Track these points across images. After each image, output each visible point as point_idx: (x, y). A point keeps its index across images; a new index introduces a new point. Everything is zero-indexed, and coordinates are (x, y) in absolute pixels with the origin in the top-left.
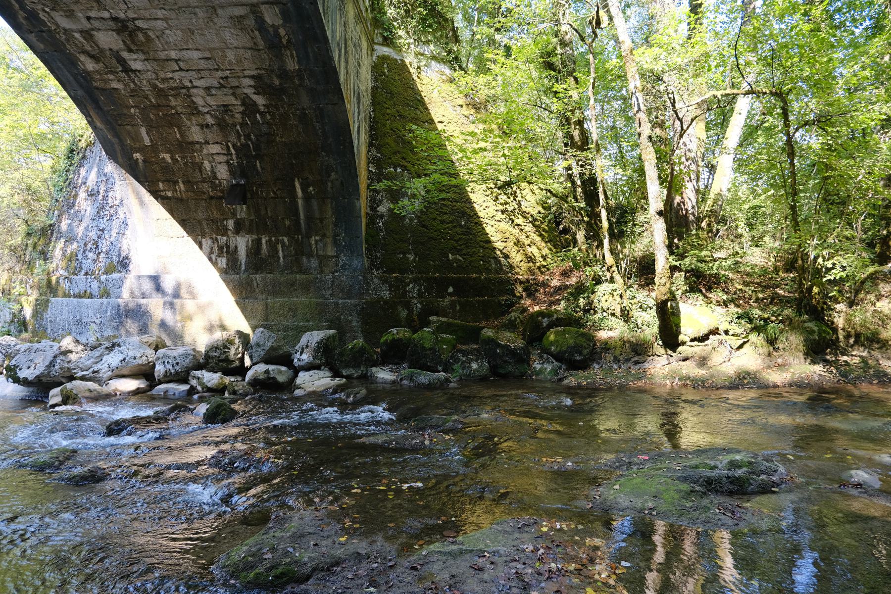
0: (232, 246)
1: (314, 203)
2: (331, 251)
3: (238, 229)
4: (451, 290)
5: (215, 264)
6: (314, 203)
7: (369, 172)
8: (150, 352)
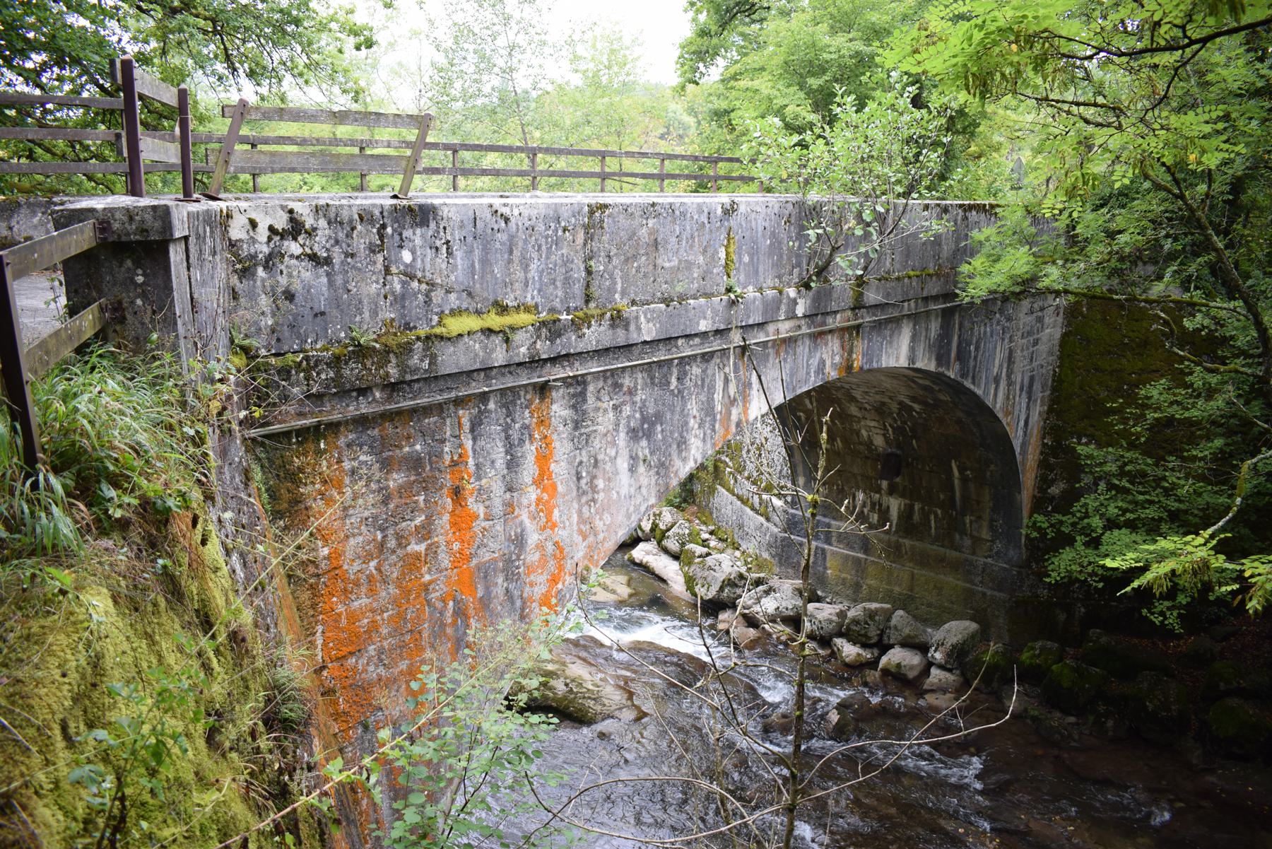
0: (884, 505)
1: (972, 486)
2: (985, 534)
3: (892, 491)
6: (972, 486)
7: (1044, 445)
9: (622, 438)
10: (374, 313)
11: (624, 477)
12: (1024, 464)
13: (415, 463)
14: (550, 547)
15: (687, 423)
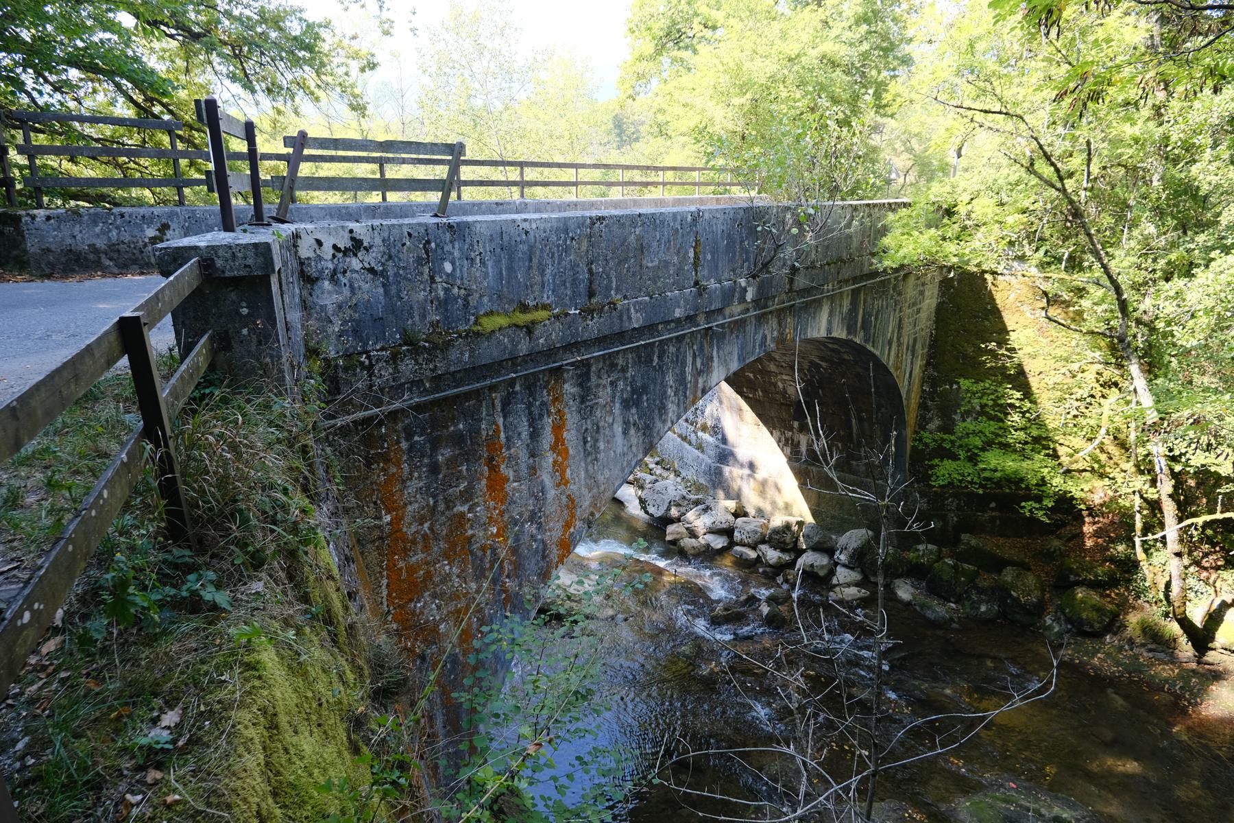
4: (993, 505)
5: (783, 450)
8: (731, 518)
10: (423, 316)
11: (619, 439)
12: (908, 406)
13: (458, 439)
15: (665, 392)
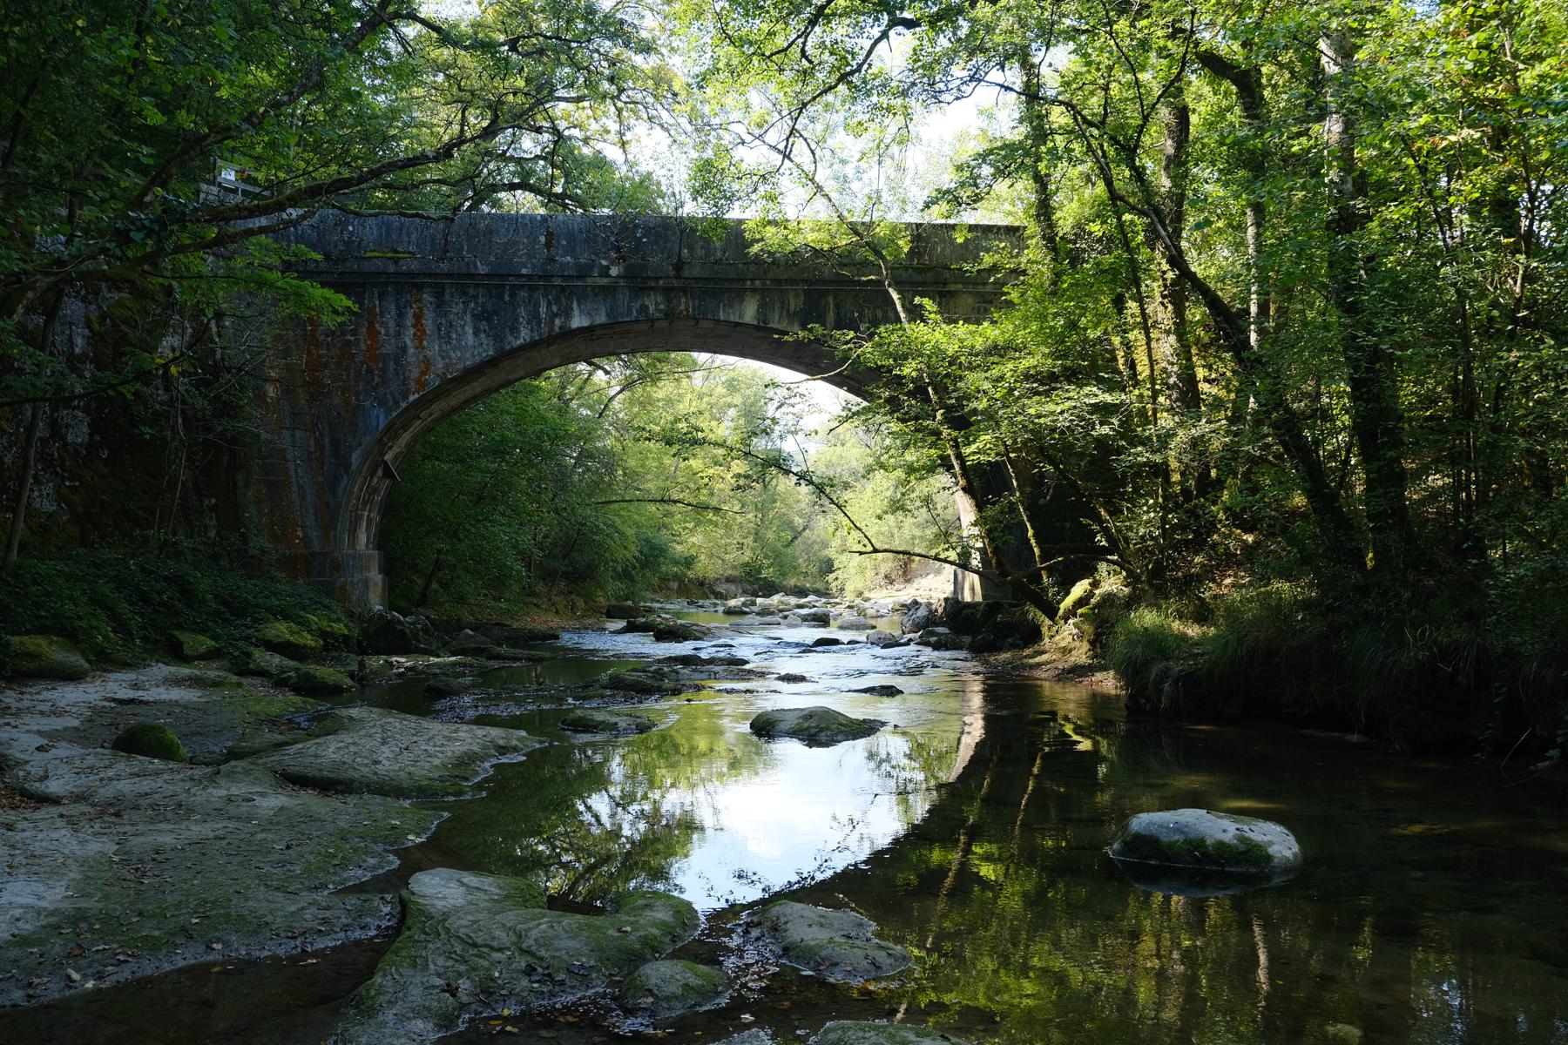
9: (468, 318)
10: (336, 246)
14: (421, 358)
